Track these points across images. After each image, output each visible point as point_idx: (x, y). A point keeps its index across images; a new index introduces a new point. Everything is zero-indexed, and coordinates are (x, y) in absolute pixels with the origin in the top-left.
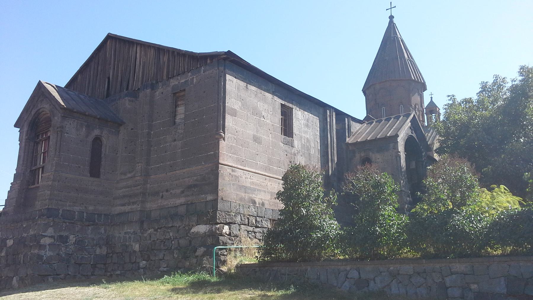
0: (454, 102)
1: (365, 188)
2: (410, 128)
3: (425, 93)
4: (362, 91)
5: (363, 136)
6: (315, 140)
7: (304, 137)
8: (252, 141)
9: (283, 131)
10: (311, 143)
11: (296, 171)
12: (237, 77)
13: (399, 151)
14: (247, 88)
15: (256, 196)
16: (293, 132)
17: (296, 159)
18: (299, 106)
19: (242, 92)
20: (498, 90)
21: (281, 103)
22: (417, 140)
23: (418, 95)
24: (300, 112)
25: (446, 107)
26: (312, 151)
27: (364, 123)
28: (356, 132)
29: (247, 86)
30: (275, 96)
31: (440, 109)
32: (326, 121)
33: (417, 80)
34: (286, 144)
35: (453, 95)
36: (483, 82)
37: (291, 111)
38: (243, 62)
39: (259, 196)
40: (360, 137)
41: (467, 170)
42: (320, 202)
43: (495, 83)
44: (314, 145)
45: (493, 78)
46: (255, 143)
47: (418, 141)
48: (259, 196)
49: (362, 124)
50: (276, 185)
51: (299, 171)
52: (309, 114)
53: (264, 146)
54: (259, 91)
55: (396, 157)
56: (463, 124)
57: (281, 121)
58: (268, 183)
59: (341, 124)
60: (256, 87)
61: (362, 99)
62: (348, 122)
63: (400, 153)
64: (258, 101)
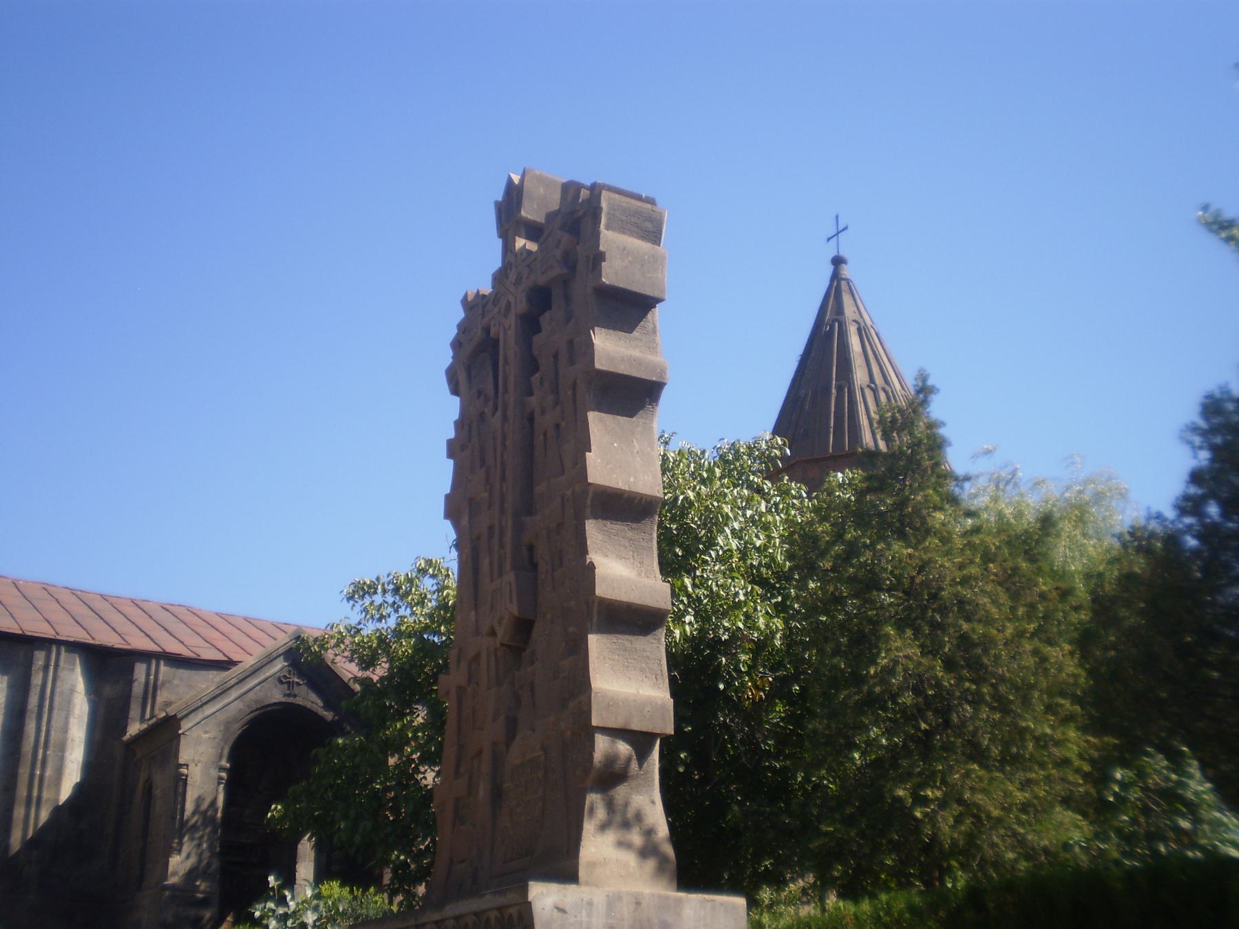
13: (181, 761)
62: (148, 675)
63: (188, 769)
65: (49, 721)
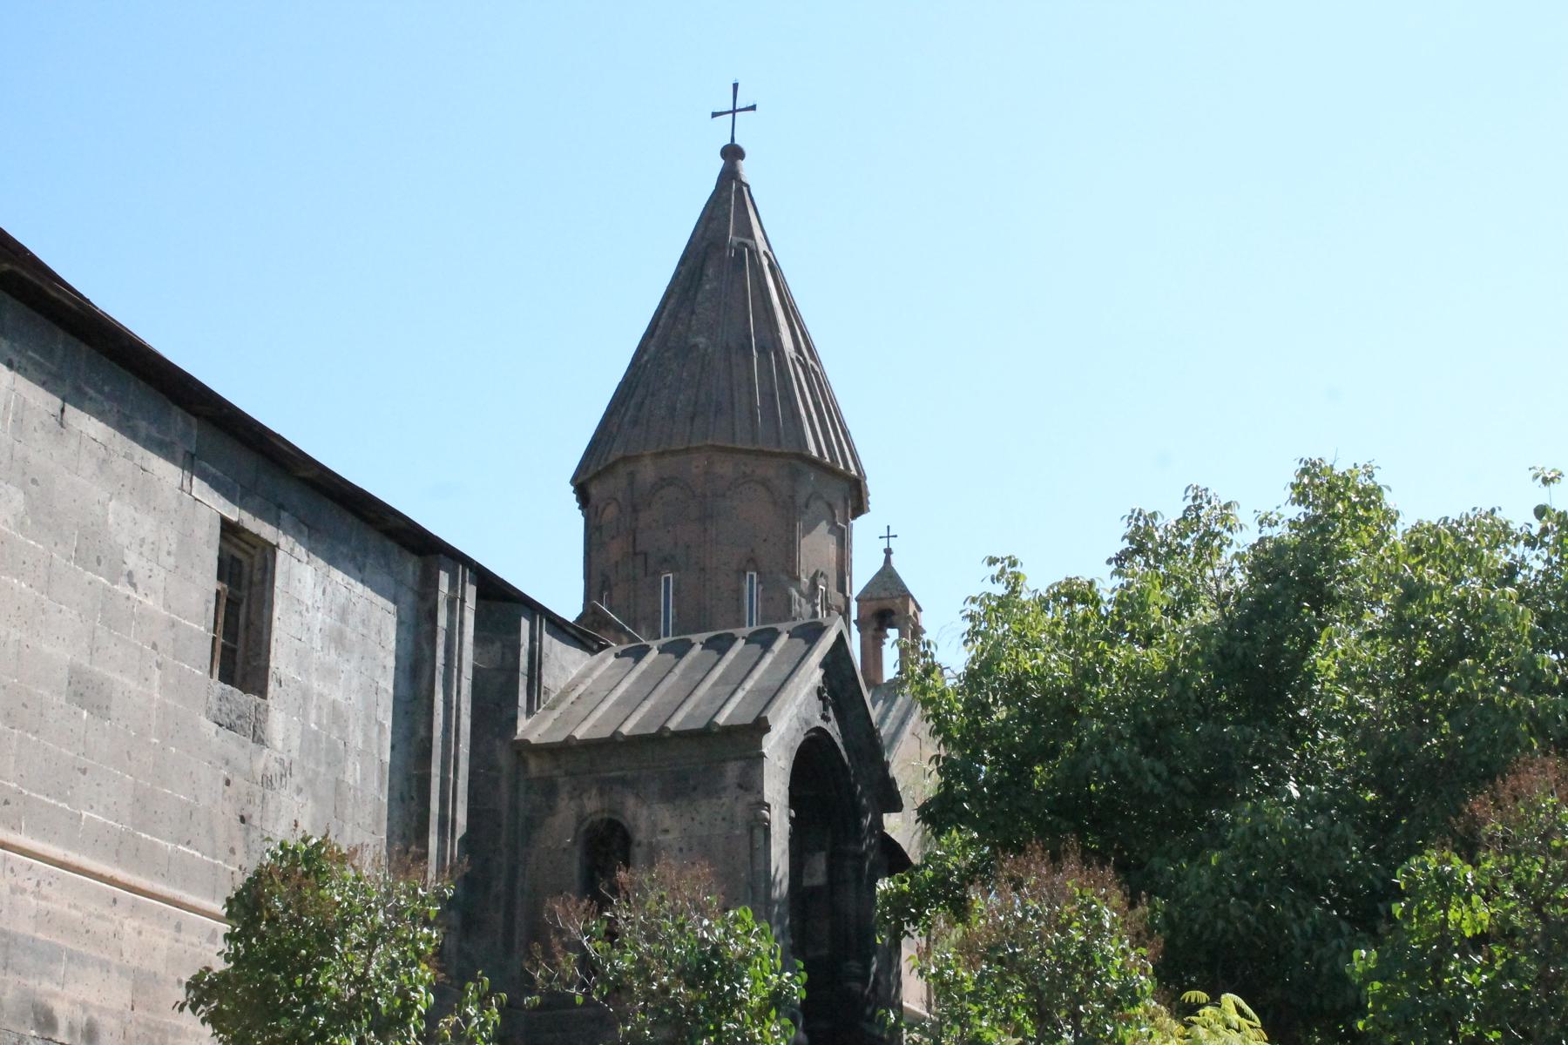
0: (1013, 591)
1: (650, 980)
2: (819, 692)
3: (860, 526)
4: (574, 481)
5: (598, 714)
6: (368, 717)
7: (320, 695)
8: (64, 703)
9: (218, 657)
10: (351, 728)
11: (306, 875)
12: (16, 364)
13: (766, 800)
14: (62, 425)
15: (58, 989)
16: (267, 667)
17: (272, 806)
18: (309, 537)
19: (36, 441)
20: (1199, 556)
21: (225, 522)
22: (844, 753)
23: (830, 532)
24: (310, 568)
25: (976, 608)
26: (349, 773)
27: (602, 648)
28: (565, 693)
29: (63, 411)
30: (198, 477)
31: (919, 608)
32: (427, 627)
33: (828, 460)
34: (230, 728)
35: (1010, 557)
36: (1140, 514)
37: (266, 559)
38: (59, 291)
39: (77, 991)
40: (585, 719)
41: (1113, 920)
42: (414, 1035)
43: (1188, 521)
44: (364, 742)
45: (1184, 499)
46: (75, 707)
47: (846, 760)
48: (77, 991)
49: (593, 652)
50: (164, 937)
51: (319, 872)
52: (352, 581)
53: (121, 727)
54: (120, 442)
55: (751, 830)
56: (1052, 695)
57: (212, 606)
58: (127, 922)
59: (498, 645)
60: (108, 424)
61: (575, 521)
64: (112, 494)
65: (459, 693)
